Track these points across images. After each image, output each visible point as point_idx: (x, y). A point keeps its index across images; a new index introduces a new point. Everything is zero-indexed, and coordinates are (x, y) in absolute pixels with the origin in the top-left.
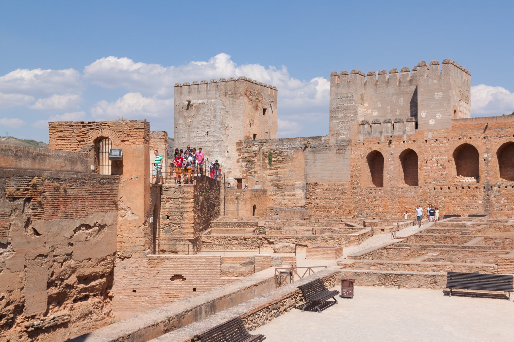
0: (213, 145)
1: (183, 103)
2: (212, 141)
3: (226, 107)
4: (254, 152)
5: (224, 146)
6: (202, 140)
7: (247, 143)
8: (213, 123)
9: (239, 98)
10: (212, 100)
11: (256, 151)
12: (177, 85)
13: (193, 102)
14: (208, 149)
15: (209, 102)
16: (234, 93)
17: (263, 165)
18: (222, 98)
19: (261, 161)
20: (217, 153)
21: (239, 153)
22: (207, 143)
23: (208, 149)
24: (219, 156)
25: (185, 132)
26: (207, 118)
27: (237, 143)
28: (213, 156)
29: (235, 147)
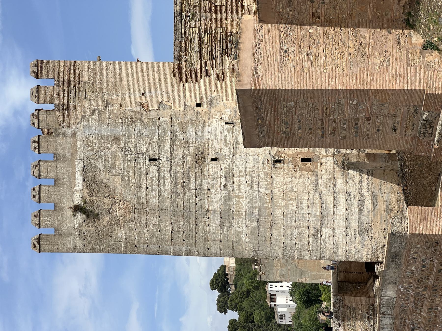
0: (181, 145)
1: (80, 226)
2: (172, 146)
3: (95, 110)
4: (201, 37)
5: (185, 115)
6: (168, 175)
7: (181, 53)
8: (130, 145)
9: (77, 74)
10: (79, 144)
11: (199, 30)
12: (36, 243)
13: (78, 201)
14: (189, 158)
15: (82, 156)
16: (65, 88)
17: (232, 12)
18: (75, 120)
19: (223, 16)
20: (199, 133)
21: (203, 74)
22: (175, 161)
23: (189, 158)
24: (207, 129)
25: (146, 223)
26: (119, 160)
27: (178, 82)
28: (207, 145)
29: (187, 85)
